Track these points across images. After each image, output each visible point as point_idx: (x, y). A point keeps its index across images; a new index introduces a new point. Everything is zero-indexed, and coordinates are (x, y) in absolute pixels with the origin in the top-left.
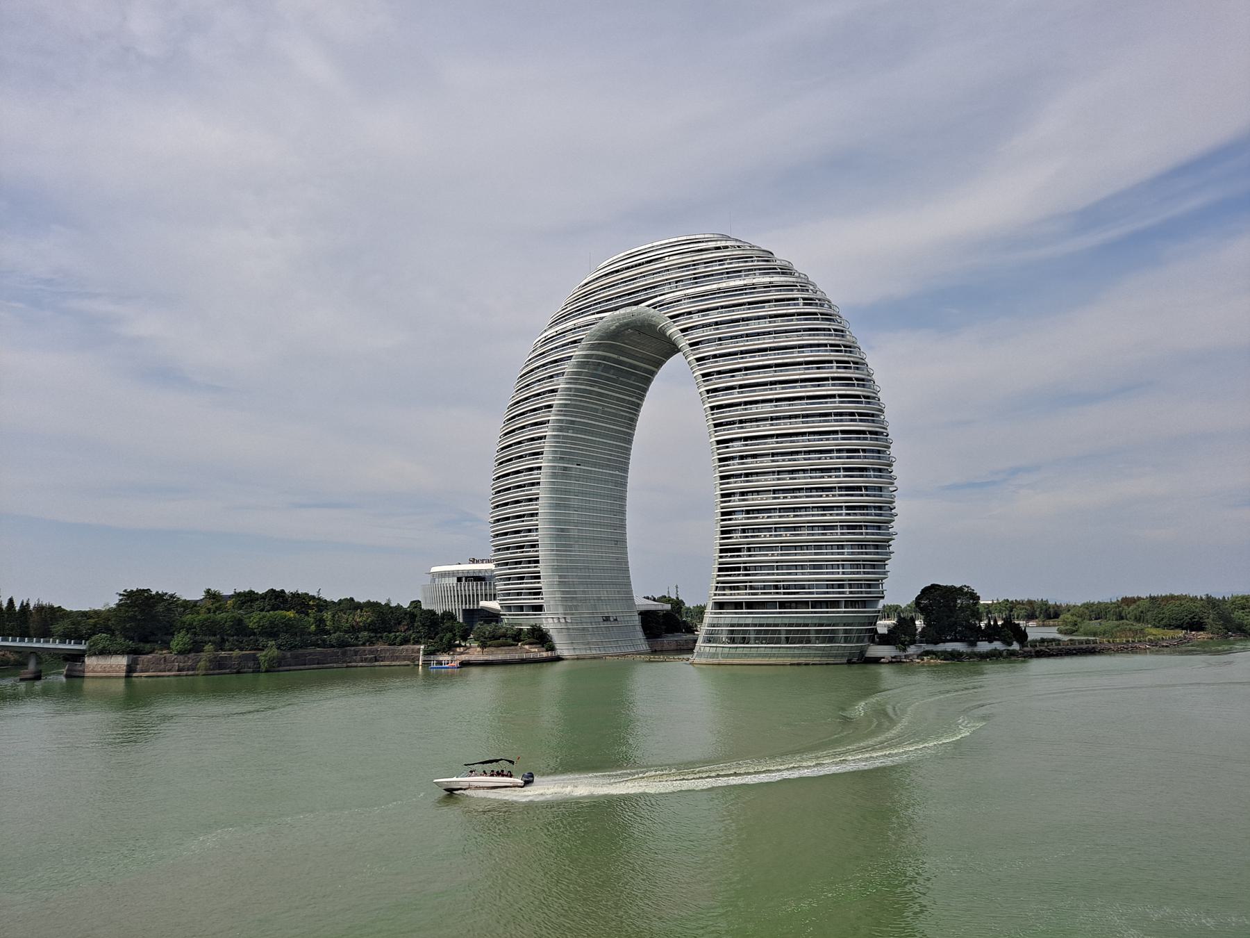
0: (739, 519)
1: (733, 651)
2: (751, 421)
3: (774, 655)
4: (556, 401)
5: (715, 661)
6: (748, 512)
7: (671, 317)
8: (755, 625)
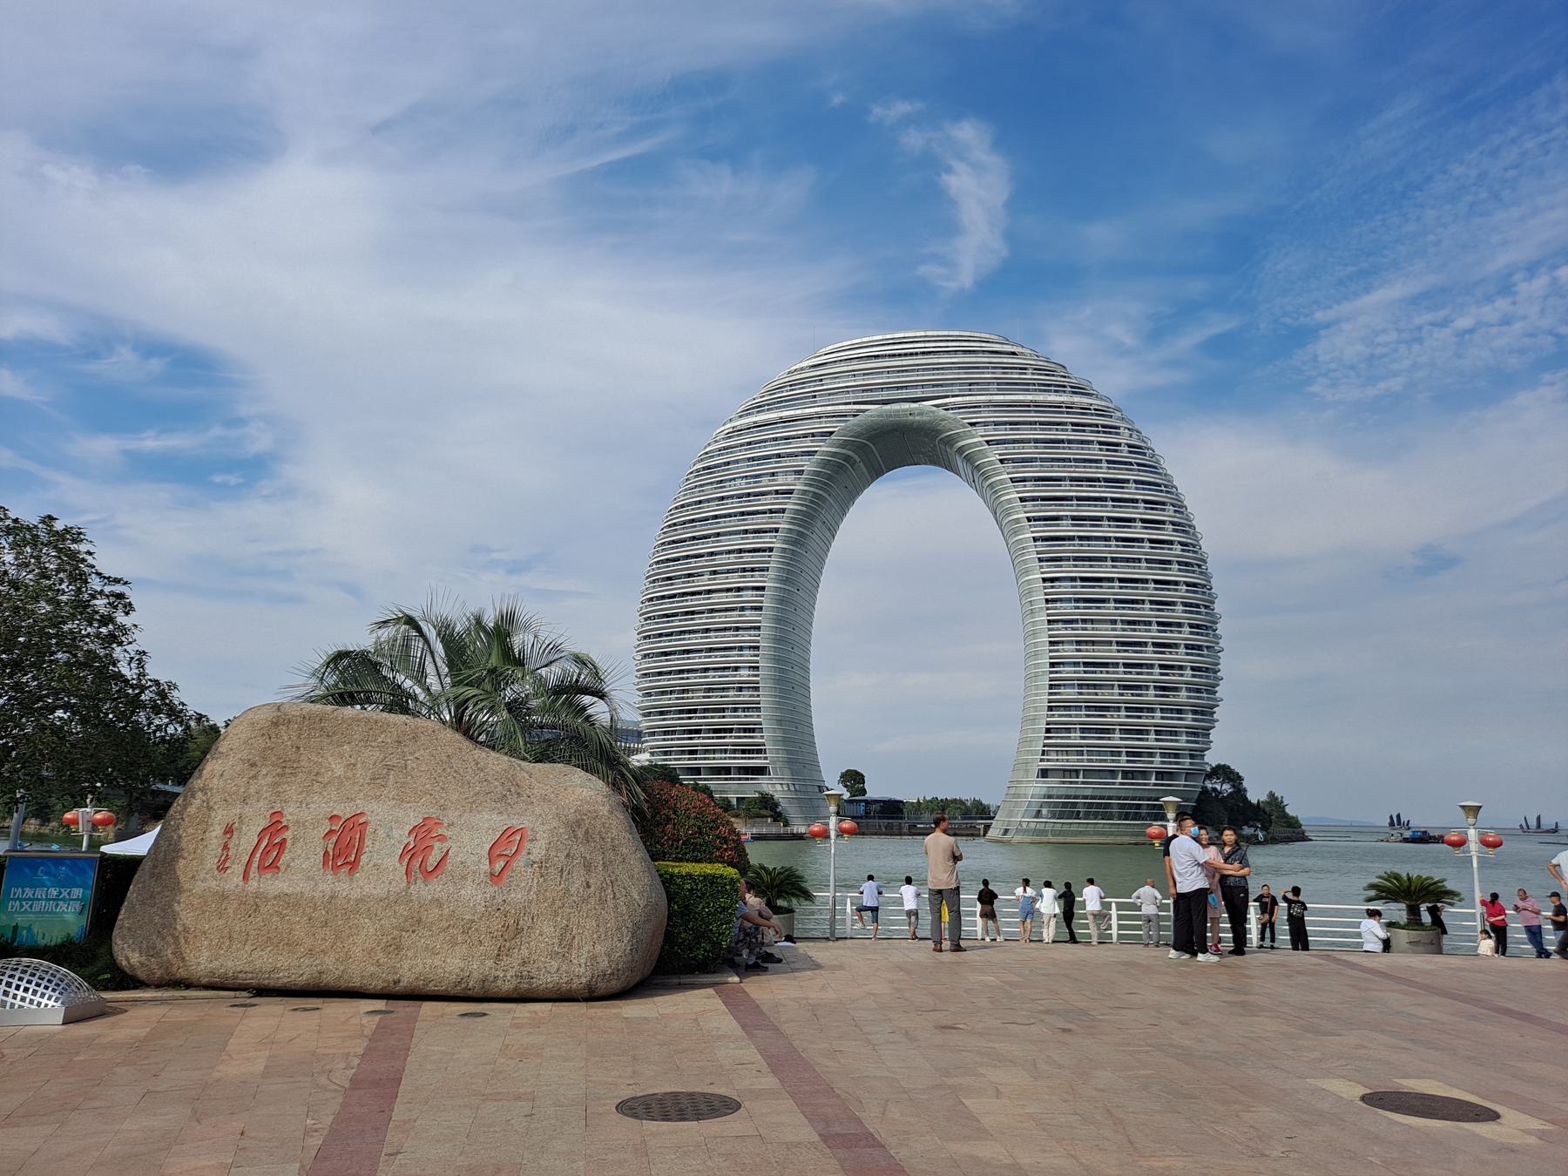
0: (1067, 672)
1: (1065, 828)
2: (1083, 559)
3: (1111, 833)
4: (791, 505)
5: (1044, 839)
6: (1085, 664)
7: (972, 424)
8: (1085, 797)
